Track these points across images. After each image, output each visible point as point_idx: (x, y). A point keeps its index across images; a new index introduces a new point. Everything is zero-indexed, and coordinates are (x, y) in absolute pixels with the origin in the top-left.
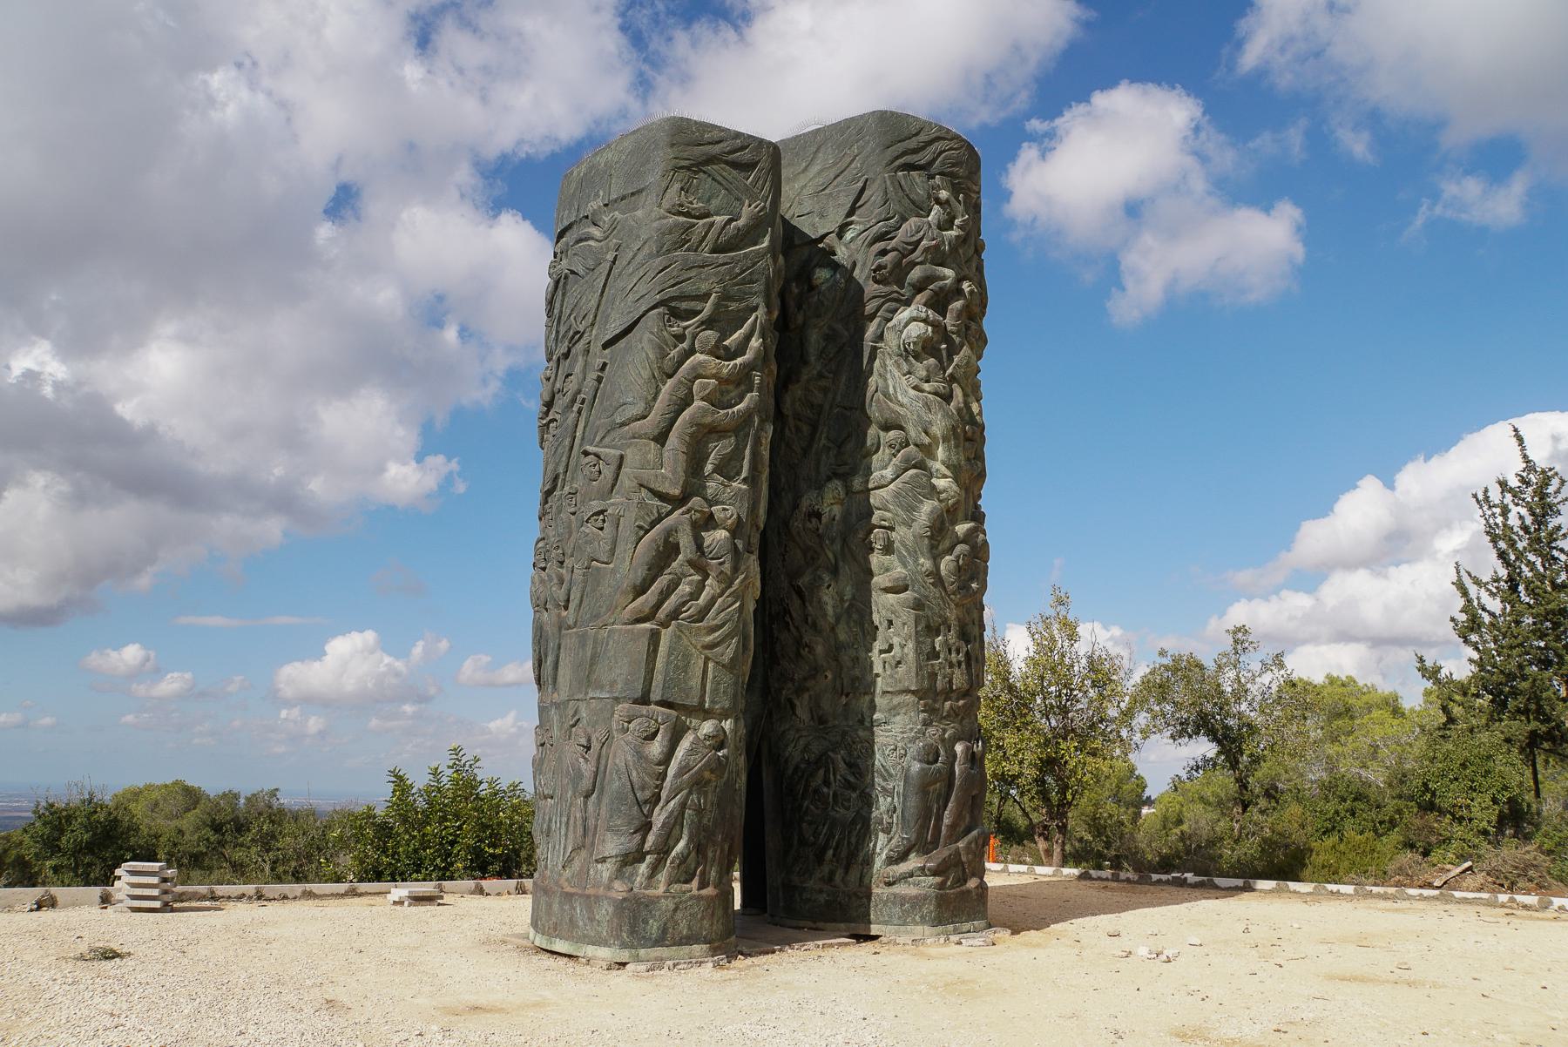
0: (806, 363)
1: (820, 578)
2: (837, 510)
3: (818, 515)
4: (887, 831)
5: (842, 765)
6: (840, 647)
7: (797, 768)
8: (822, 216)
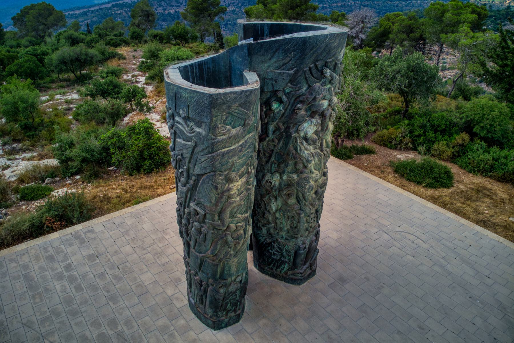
0: (268, 136)
1: (271, 200)
2: (277, 183)
3: (271, 183)
4: (289, 264)
5: (276, 247)
6: (276, 218)
7: (263, 242)
8: (276, 82)
